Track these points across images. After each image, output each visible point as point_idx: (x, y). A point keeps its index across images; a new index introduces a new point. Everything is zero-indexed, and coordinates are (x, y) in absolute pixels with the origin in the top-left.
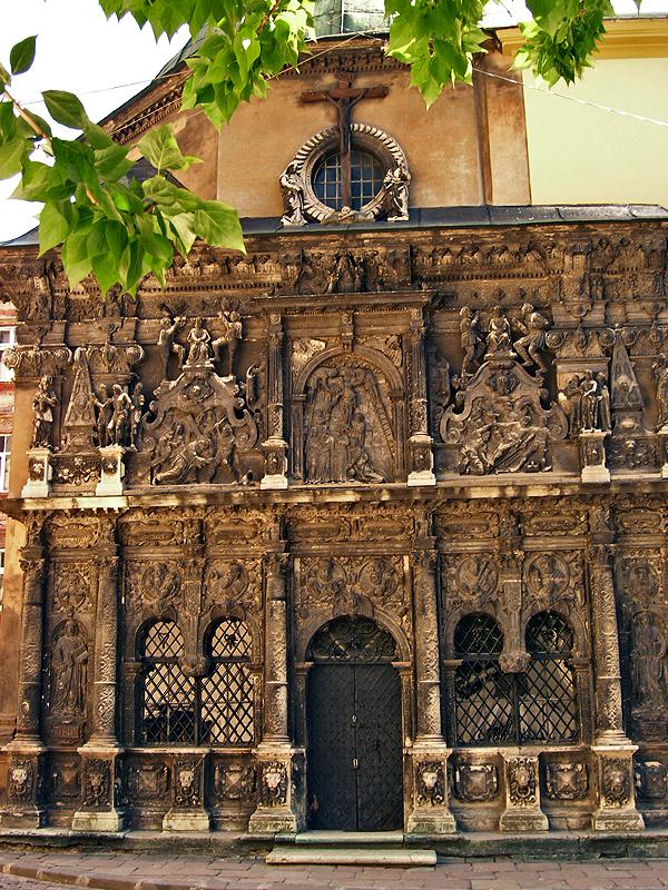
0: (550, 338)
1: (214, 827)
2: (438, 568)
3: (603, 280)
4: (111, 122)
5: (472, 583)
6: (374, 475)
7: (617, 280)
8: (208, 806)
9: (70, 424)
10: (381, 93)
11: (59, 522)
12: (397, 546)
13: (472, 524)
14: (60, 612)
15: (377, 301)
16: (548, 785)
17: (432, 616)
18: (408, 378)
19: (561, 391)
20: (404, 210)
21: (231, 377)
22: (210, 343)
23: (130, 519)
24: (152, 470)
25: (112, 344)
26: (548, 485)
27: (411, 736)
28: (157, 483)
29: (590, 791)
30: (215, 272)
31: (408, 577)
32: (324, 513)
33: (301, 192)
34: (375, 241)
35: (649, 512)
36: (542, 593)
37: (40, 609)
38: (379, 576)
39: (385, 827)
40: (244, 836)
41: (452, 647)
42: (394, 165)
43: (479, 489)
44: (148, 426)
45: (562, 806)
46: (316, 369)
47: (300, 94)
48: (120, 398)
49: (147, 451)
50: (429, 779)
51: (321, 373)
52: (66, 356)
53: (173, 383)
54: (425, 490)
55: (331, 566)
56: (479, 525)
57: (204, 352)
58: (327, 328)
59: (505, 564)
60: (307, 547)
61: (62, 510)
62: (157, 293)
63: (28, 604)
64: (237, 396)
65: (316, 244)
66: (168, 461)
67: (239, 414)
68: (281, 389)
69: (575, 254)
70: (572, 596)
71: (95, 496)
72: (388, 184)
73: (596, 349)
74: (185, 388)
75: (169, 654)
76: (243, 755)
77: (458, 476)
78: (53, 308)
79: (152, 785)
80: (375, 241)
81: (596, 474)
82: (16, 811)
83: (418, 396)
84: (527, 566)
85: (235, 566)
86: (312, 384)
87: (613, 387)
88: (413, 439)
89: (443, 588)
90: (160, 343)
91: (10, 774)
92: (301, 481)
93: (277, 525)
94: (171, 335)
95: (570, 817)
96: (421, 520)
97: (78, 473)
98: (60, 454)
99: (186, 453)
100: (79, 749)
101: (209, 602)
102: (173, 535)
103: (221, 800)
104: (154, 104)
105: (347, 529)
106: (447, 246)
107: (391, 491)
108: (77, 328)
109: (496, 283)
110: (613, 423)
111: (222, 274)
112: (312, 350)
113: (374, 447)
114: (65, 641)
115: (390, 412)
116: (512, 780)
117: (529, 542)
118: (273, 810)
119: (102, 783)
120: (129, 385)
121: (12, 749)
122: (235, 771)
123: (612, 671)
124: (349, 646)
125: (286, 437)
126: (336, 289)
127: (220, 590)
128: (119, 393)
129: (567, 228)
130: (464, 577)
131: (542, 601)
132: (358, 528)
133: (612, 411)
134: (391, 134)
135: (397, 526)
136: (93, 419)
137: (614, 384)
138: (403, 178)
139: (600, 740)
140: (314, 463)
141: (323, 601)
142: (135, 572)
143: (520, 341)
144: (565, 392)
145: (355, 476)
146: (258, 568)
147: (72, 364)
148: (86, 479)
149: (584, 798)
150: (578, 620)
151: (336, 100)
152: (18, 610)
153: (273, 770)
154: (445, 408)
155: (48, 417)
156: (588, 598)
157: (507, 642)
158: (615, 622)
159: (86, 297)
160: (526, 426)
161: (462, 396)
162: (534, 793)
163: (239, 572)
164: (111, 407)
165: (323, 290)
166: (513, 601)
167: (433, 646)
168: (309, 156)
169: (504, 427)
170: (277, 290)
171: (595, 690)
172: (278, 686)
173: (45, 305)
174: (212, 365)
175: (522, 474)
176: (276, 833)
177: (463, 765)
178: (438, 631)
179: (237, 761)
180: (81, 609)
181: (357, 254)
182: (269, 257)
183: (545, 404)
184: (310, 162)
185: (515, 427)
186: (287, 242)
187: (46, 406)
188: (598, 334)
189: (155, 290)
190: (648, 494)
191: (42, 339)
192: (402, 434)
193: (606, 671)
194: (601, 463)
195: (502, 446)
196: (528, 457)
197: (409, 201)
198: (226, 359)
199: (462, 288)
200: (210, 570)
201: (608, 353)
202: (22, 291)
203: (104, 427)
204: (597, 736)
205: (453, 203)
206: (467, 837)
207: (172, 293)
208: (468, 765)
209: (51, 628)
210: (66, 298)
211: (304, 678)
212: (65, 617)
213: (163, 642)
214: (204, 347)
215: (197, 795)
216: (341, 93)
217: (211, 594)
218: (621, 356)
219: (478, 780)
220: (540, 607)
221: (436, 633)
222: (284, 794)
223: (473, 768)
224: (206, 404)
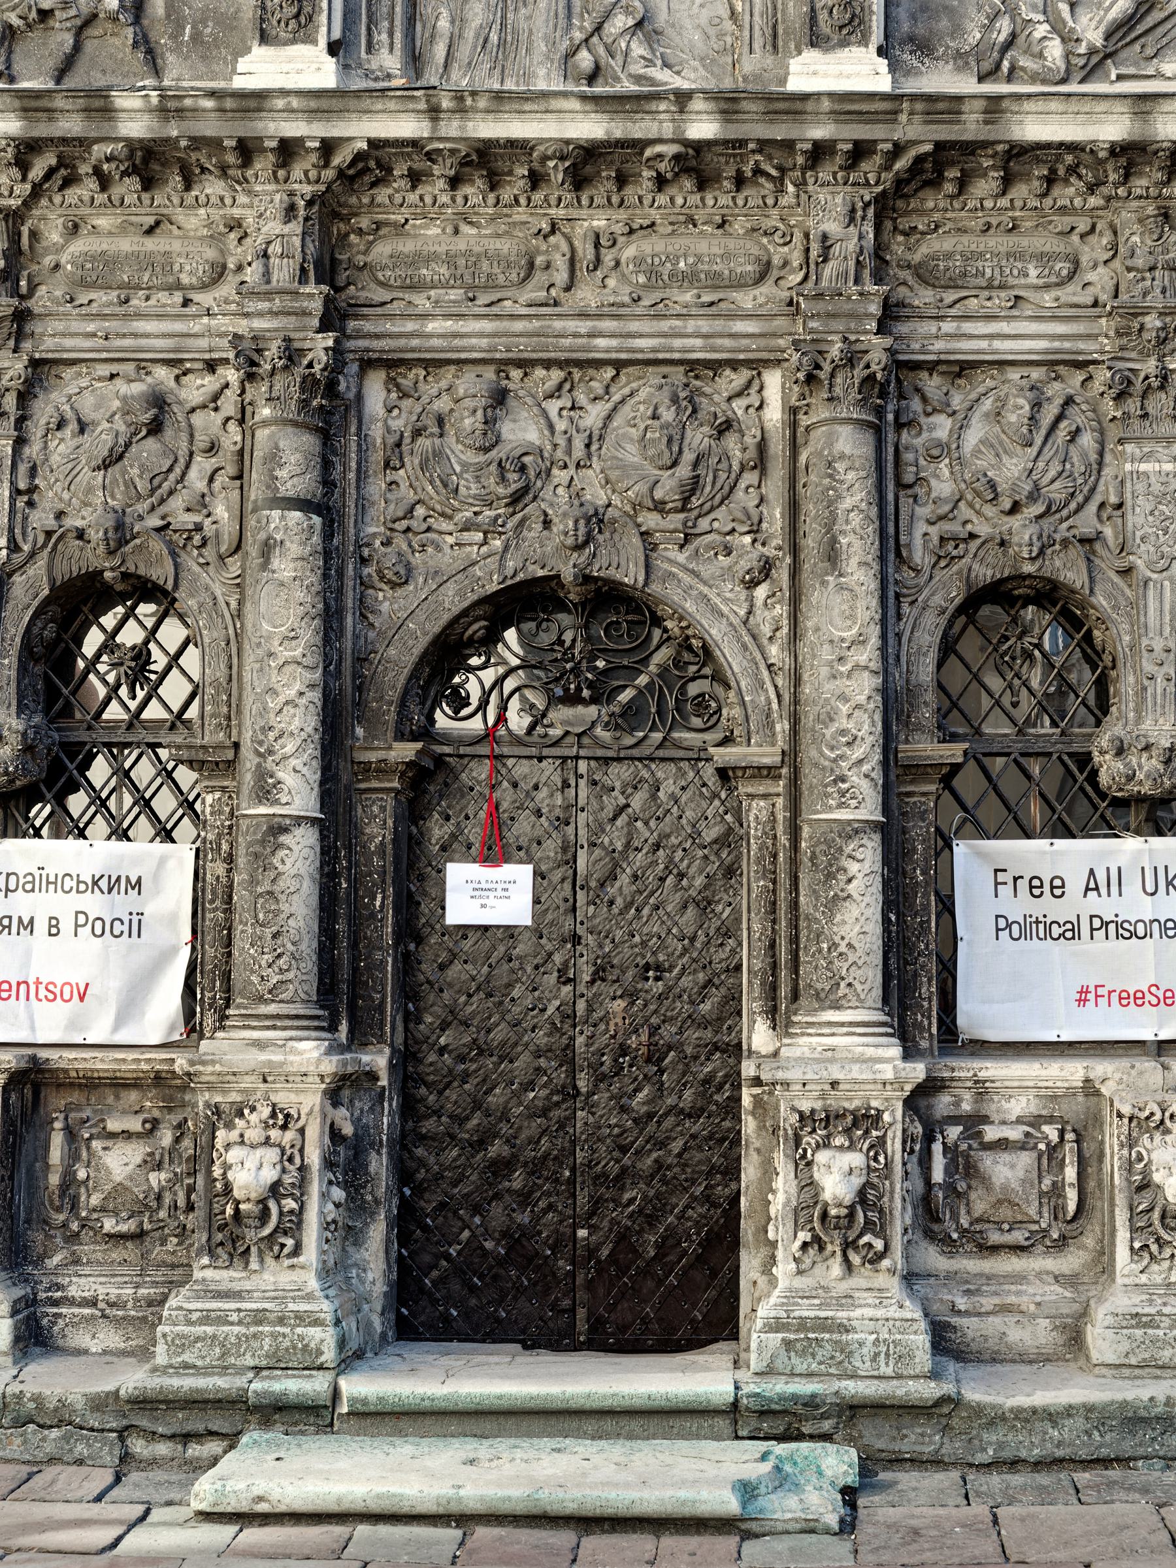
2: (892, 396)
5: (1011, 470)
12: (740, 326)
31: (778, 448)
38: (675, 440)
56: (1044, 258)
59: (1132, 405)
93: (296, 227)
96: (833, 227)
101: (41, 519)
103: (73, 1238)
105: (561, 263)
122: (127, 1135)
130: (978, 446)
132: (598, 262)
157: (1126, 685)
178: (884, 636)
200: (43, 411)
217: (51, 496)
219: (1007, 1171)
221: (874, 641)
222: (293, 1224)
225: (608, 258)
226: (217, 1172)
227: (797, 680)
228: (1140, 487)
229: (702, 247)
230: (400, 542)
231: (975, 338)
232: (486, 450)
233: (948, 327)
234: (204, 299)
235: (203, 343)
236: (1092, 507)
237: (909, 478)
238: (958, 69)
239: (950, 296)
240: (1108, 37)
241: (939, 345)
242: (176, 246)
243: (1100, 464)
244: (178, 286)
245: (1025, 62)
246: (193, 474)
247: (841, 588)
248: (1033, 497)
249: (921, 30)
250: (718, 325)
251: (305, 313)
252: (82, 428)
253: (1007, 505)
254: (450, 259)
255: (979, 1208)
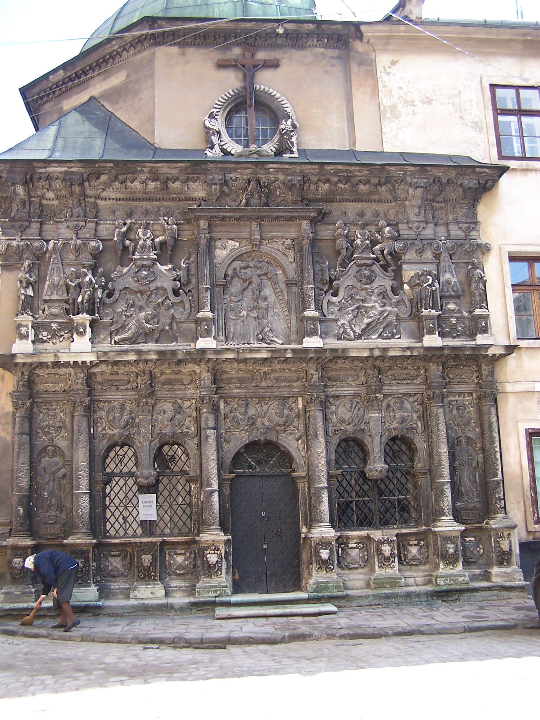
0: (398, 245)
1: (167, 594)
3: (433, 207)
4: (61, 72)
5: (347, 416)
6: (275, 339)
7: (441, 208)
8: (161, 580)
9: (48, 298)
10: (275, 65)
11: (40, 372)
13: (348, 375)
14: (42, 440)
15: (278, 214)
16: (402, 555)
17: (322, 439)
18: (301, 271)
19: (406, 283)
20: (295, 149)
21: (170, 266)
22: (153, 240)
23: (96, 370)
24: (111, 334)
25: (78, 239)
26: (403, 348)
27: (306, 525)
28: (116, 343)
29: (429, 559)
30: (156, 188)
32: (242, 366)
33: (219, 132)
34: (278, 170)
35: (466, 368)
36: (395, 424)
37: (28, 438)
39: (286, 590)
40: (193, 600)
41: (334, 461)
42: (288, 117)
43: (355, 350)
44: (108, 301)
45: (410, 570)
46: (233, 260)
47: (216, 60)
48: (87, 279)
49: (107, 320)
50: (324, 554)
51: (237, 264)
52: (42, 247)
53: (126, 269)
54: (318, 350)
55: (247, 405)
56: (352, 376)
57: (149, 247)
58: (241, 232)
59: (370, 403)
60: (230, 391)
61: (45, 363)
62: (111, 202)
63: (19, 434)
64: (175, 280)
65: (235, 170)
66: (124, 326)
67: (176, 293)
68: (208, 275)
69: (417, 187)
70: (415, 425)
71: (70, 352)
72: (283, 130)
73: (429, 255)
74: (136, 273)
75: (125, 470)
76: (186, 543)
77: (336, 341)
78: (30, 209)
79: (119, 566)
80: (278, 170)
81: (433, 341)
82: (16, 590)
83: (308, 283)
84: (384, 404)
85: (176, 405)
86: (230, 272)
87: (441, 281)
88: (306, 313)
89: (326, 420)
90: (115, 239)
91: (11, 562)
92: (224, 343)
94: (124, 233)
95: (417, 577)
96: (313, 372)
97: (54, 335)
98: (39, 320)
99: (138, 321)
100: (65, 541)
102: (129, 382)
104: (99, 60)
105: (259, 378)
106: (328, 176)
107: (294, 351)
108: (49, 227)
109: (359, 206)
110: (442, 306)
111: (162, 189)
112: (229, 248)
113: (275, 319)
114: (45, 461)
115: (286, 295)
116: (380, 552)
117: (386, 388)
118: (212, 580)
119: (84, 566)
120: (92, 270)
121: (11, 543)
123: (447, 479)
124: (259, 463)
125: (212, 311)
126: (247, 204)
127: (166, 422)
128: (86, 275)
129: (412, 168)
131: (395, 429)
133: (441, 298)
134: (283, 95)
135: (295, 376)
136: (66, 294)
137: (442, 279)
138: (294, 126)
139: (439, 524)
140: (232, 330)
141: (242, 430)
142: (101, 409)
143: (377, 247)
144: (409, 284)
145: (263, 340)
146: (193, 407)
147: (46, 252)
148: (61, 339)
149: (425, 564)
150: (420, 443)
151: (244, 66)
152: (9, 439)
153: (213, 552)
154: (326, 292)
155: (30, 292)
156: (427, 427)
158: (446, 443)
159: (55, 202)
160: (382, 307)
161: (338, 284)
162: (394, 562)
163: (179, 410)
164: (79, 286)
165: (237, 204)
166: (376, 428)
167: (323, 461)
168: (223, 106)
169: (368, 307)
170: (203, 203)
171: (432, 490)
172: (212, 492)
173: (24, 207)
174: (155, 257)
175: (380, 340)
176: (216, 597)
177: (342, 544)
179: (182, 547)
180: (59, 437)
181: (264, 179)
182: (199, 178)
183: (394, 291)
184: (224, 110)
185: (375, 307)
186: (213, 168)
187: (29, 284)
188: (431, 244)
189: (109, 199)
190: (467, 355)
191: (22, 232)
192: (296, 310)
193: (441, 476)
194: (435, 334)
195: (366, 321)
196: (384, 328)
197: (297, 144)
198: (166, 251)
199: (335, 208)
201: (437, 256)
202: (5, 196)
203: (74, 300)
204: (435, 520)
205: (328, 146)
206: (349, 592)
207: (122, 202)
208: (347, 544)
209: (36, 452)
210: (40, 202)
211: (228, 486)
212: (47, 444)
213: (121, 461)
214: (149, 242)
215: (154, 572)
216: (247, 61)
218: (446, 260)
220: (394, 433)
222: (220, 569)
223: (350, 546)
224: (151, 285)
225: (268, 377)
226: (205, 559)
227: (308, 459)
228: (372, 419)
229: (286, 375)
230: (228, 433)
231: (341, 391)
232: (245, 415)
233: (334, 389)
234: (189, 387)
235: (189, 395)
236: (363, 423)
237: (328, 419)
238: (333, 338)
239: (335, 383)
240: (361, 331)
241: (332, 393)
242: (183, 377)
243: (364, 414)
244: (184, 384)
245: (346, 336)
246: (187, 421)
247: (318, 442)
248: (352, 422)
249: (326, 330)
250: (290, 390)
251: (213, 391)
252: (164, 414)
253: (347, 423)
254: (237, 378)
255: (348, 560)
